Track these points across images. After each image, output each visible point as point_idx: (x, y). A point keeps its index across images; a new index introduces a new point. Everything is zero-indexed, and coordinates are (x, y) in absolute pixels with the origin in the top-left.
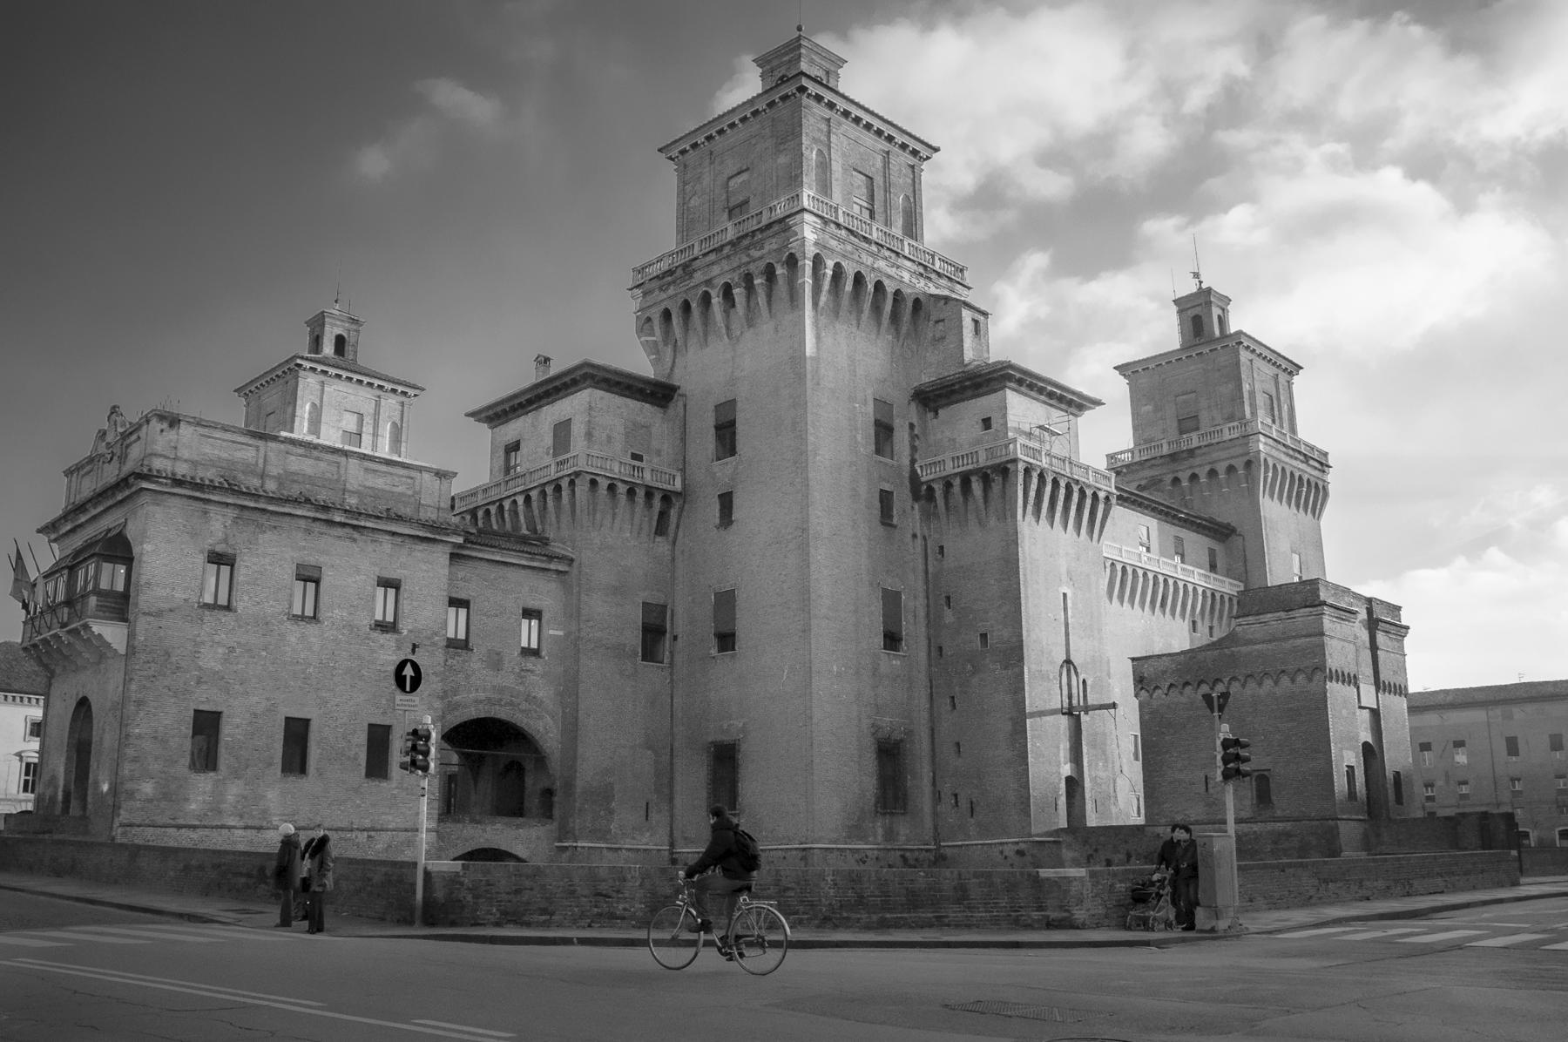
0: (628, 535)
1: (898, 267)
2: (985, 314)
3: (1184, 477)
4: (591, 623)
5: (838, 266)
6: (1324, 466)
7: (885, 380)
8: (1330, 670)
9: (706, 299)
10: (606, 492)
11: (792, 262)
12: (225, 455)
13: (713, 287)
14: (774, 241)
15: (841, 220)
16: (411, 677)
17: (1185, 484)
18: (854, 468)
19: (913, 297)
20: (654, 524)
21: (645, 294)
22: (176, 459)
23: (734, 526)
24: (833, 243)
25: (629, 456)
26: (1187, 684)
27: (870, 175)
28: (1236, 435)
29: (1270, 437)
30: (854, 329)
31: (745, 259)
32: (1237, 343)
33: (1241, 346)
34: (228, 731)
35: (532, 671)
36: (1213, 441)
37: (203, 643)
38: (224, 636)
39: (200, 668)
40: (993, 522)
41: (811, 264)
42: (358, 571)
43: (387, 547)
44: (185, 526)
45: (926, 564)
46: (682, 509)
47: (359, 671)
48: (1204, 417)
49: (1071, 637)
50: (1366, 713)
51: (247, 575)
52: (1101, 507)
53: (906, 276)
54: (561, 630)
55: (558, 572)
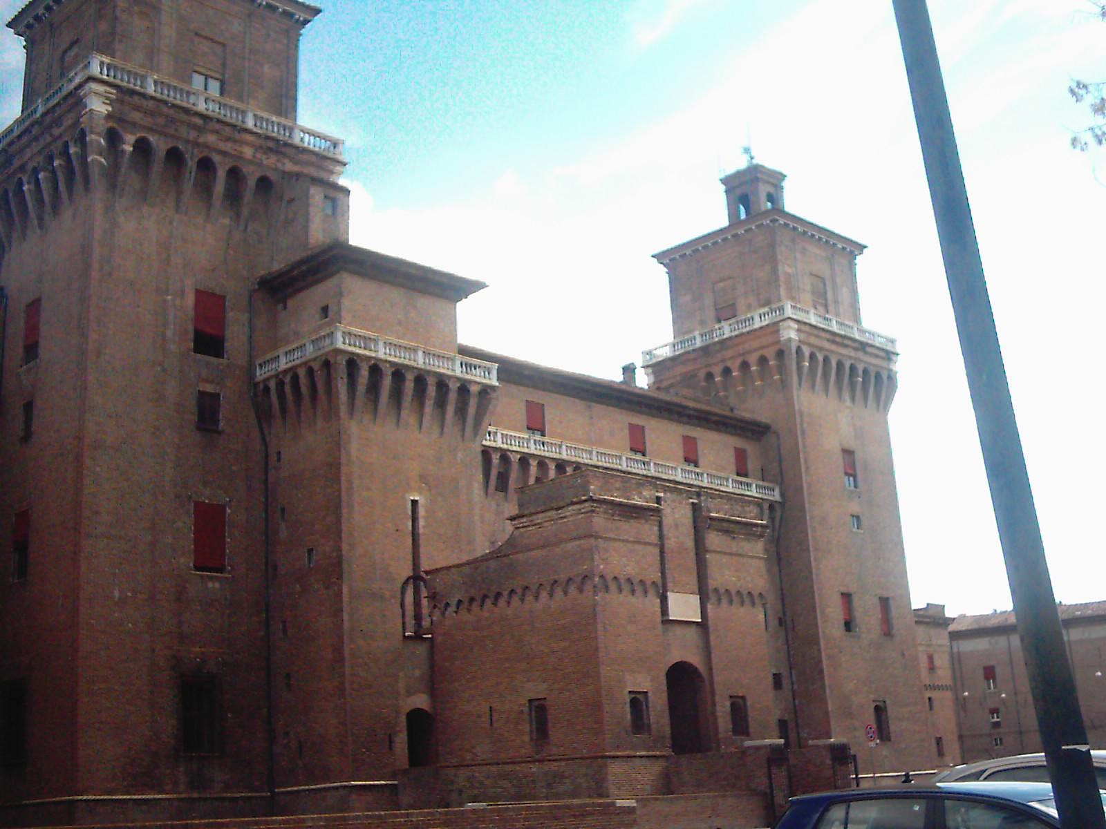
1: (235, 141)
2: (346, 192)
6: (889, 355)
7: (213, 270)
17: (718, 379)
19: (258, 174)
26: (472, 600)
27: (221, 40)
28: (766, 323)
29: (805, 323)
31: (49, 139)
32: (771, 221)
33: (777, 224)
36: (744, 330)
48: (741, 304)
53: (248, 152)
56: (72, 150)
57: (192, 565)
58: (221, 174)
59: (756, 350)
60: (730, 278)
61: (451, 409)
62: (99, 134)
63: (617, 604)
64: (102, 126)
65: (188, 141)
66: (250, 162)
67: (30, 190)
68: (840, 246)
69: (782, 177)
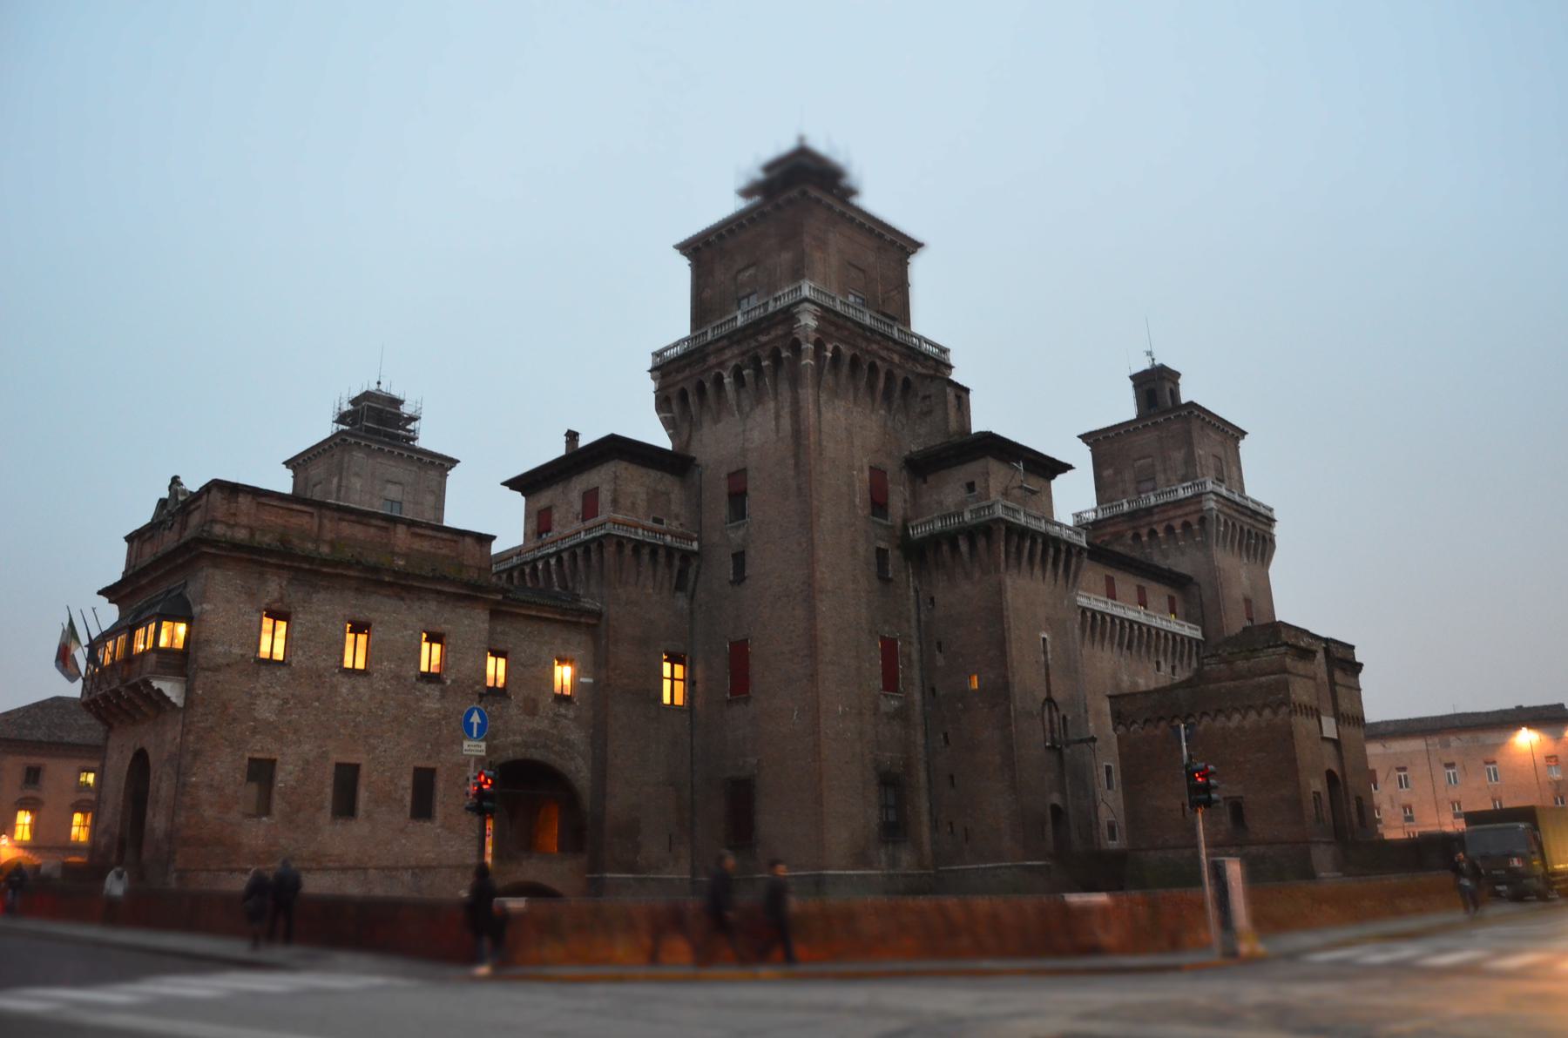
0: (651, 591)
1: (888, 349)
2: (967, 391)
3: (1144, 531)
4: (618, 672)
5: (836, 351)
6: (1270, 521)
8: (1294, 704)
9: (719, 380)
10: (630, 553)
11: (796, 347)
12: (280, 521)
13: (725, 369)
14: (780, 327)
15: (839, 308)
16: (478, 724)
17: (1145, 539)
18: (853, 529)
20: (674, 581)
21: (663, 376)
22: (236, 525)
23: (747, 581)
24: (832, 329)
25: (651, 519)
26: (1161, 718)
28: (1190, 494)
30: (851, 406)
31: (753, 344)
32: (1188, 413)
34: (284, 777)
35: (565, 717)
36: (1169, 500)
37: (259, 695)
38: (278, 689)
39: (255, 719)
40: (977, 575)
41: (813, 347)
42: (405, 627)
43: (433, 605)
44: (242, 587)
45: (919, 614)
46: (699, 567)
47: (406, 719)
48: (1161, 478)
49: (1051, 678)
50: (1329, 748)
51: (301, 631)
52: (1074, 560)
53: (896, 358)
54: (590, 677)
55: (588, 625)
56: (785, 354)
57: (881, 686)
58: (882, 376)
59: (1180, 516)
60: (1151, 456)
61: (1049, 566)
62: (811, 343)
63: (1303, 724)
64: (813, 336)
65: (862, 349)
66: (899, 366)
67: (730, 383)
68: (1230, 432)
69: (1177, 375)
